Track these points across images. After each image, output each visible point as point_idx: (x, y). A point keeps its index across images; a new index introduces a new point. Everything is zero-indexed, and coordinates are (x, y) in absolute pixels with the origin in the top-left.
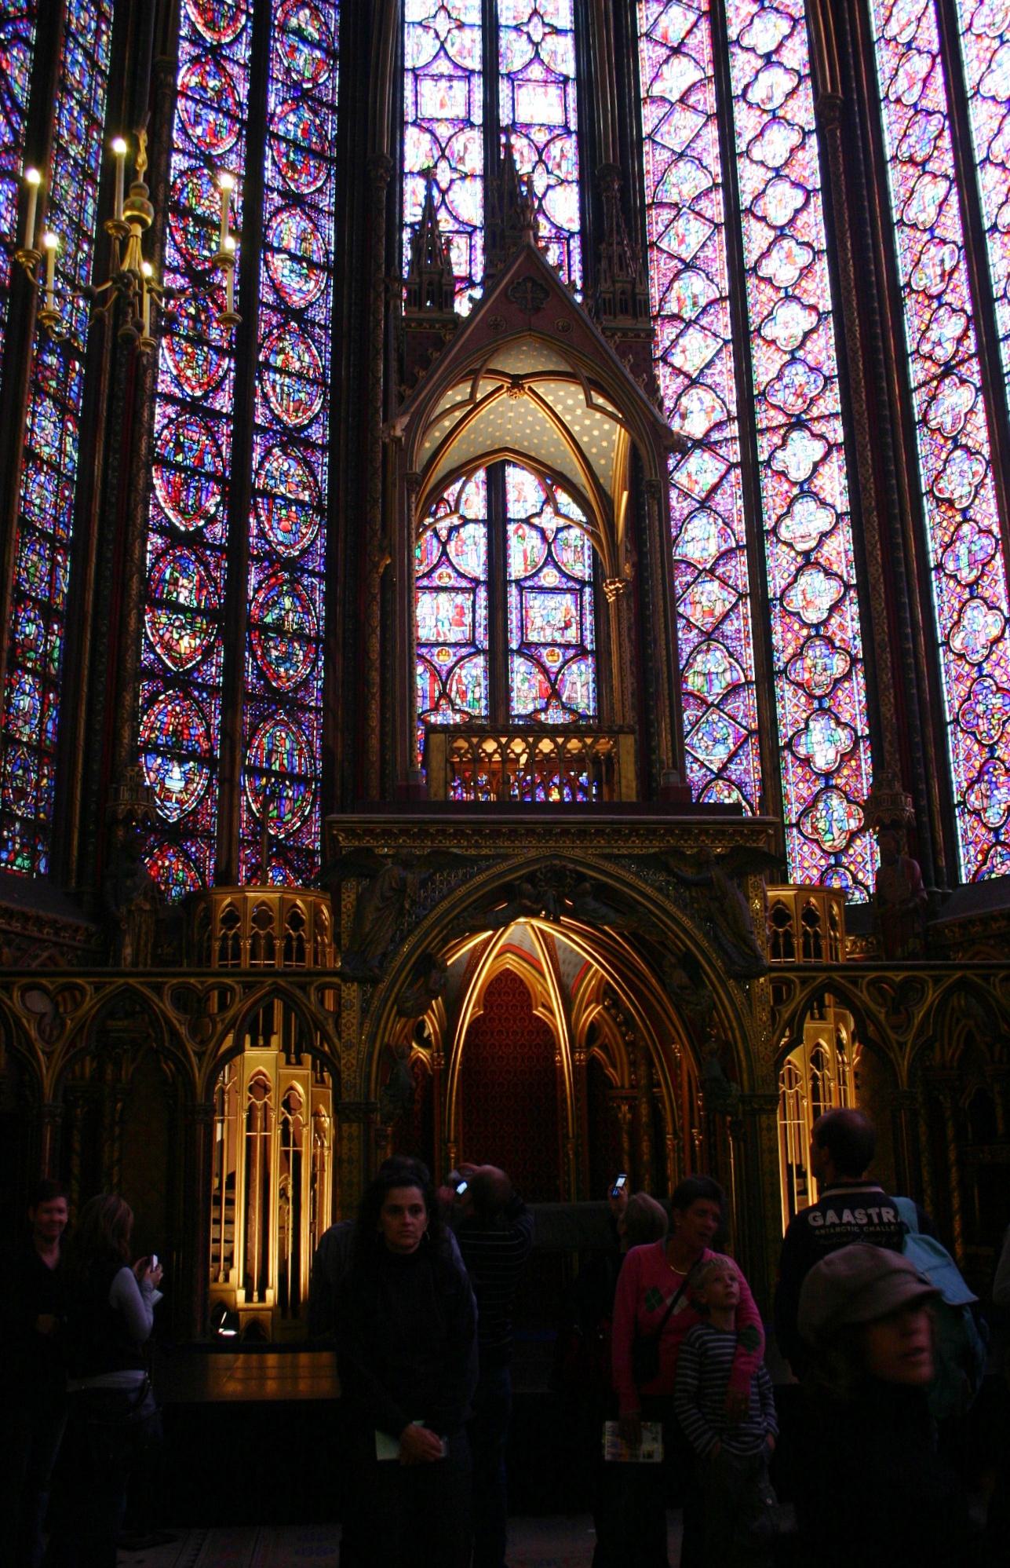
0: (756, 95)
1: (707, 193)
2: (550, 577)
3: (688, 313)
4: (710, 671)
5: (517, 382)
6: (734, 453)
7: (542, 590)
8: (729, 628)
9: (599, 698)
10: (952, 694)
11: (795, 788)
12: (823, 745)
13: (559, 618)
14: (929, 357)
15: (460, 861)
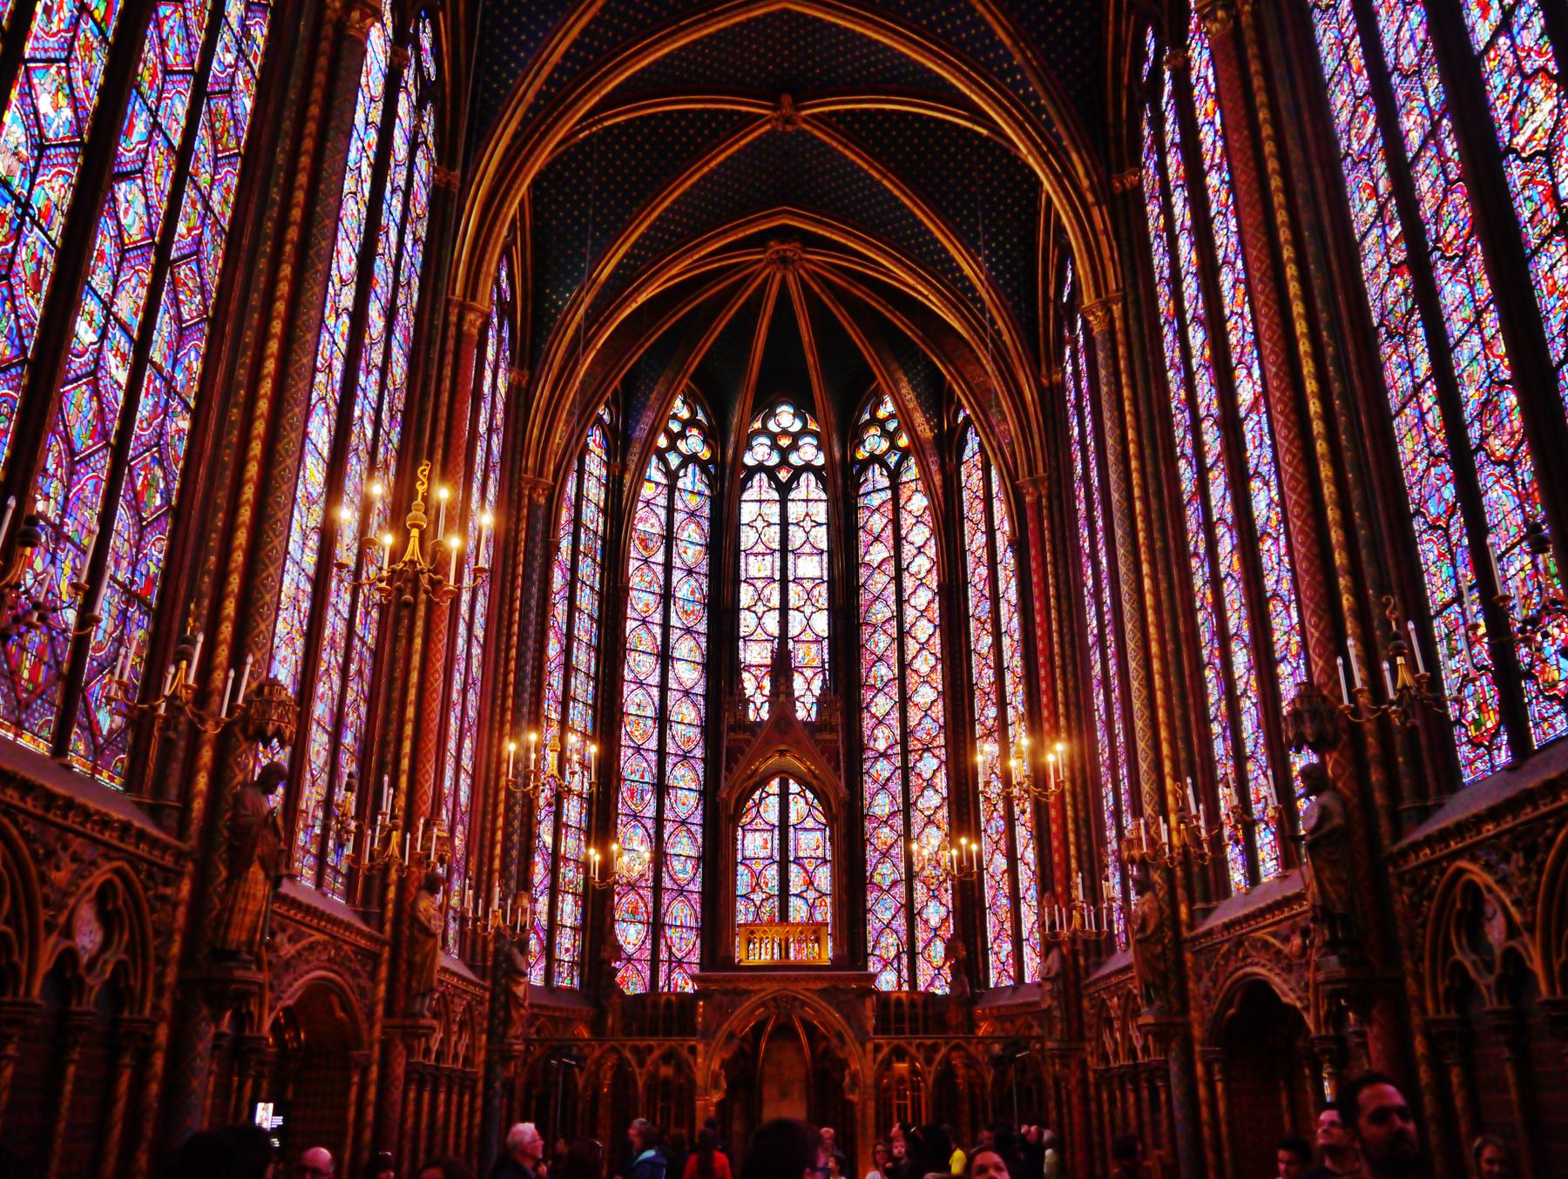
0: (913, 569)
1: (889, 620)
2: (810, 823)
3: (879, 685)
4: (885, 873)
5: (782, 753)
6: (898, 762)
7: (805, 829)
8: (893, 852)
9: (833, 885)
10: (988, 894)
11: (921, 935)
12: (934, 913)
13: (813, 845)
14: (983, 724)
15: (748, 992)
